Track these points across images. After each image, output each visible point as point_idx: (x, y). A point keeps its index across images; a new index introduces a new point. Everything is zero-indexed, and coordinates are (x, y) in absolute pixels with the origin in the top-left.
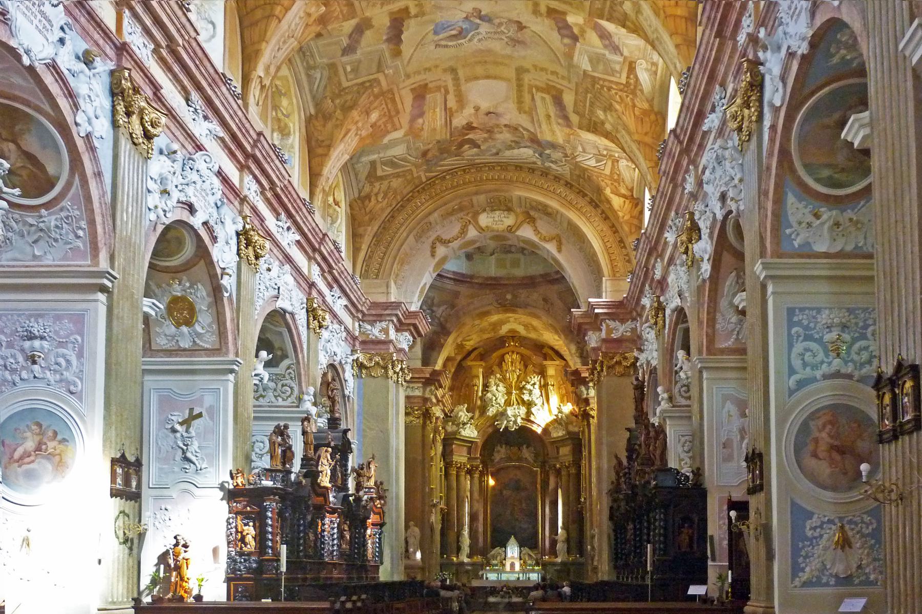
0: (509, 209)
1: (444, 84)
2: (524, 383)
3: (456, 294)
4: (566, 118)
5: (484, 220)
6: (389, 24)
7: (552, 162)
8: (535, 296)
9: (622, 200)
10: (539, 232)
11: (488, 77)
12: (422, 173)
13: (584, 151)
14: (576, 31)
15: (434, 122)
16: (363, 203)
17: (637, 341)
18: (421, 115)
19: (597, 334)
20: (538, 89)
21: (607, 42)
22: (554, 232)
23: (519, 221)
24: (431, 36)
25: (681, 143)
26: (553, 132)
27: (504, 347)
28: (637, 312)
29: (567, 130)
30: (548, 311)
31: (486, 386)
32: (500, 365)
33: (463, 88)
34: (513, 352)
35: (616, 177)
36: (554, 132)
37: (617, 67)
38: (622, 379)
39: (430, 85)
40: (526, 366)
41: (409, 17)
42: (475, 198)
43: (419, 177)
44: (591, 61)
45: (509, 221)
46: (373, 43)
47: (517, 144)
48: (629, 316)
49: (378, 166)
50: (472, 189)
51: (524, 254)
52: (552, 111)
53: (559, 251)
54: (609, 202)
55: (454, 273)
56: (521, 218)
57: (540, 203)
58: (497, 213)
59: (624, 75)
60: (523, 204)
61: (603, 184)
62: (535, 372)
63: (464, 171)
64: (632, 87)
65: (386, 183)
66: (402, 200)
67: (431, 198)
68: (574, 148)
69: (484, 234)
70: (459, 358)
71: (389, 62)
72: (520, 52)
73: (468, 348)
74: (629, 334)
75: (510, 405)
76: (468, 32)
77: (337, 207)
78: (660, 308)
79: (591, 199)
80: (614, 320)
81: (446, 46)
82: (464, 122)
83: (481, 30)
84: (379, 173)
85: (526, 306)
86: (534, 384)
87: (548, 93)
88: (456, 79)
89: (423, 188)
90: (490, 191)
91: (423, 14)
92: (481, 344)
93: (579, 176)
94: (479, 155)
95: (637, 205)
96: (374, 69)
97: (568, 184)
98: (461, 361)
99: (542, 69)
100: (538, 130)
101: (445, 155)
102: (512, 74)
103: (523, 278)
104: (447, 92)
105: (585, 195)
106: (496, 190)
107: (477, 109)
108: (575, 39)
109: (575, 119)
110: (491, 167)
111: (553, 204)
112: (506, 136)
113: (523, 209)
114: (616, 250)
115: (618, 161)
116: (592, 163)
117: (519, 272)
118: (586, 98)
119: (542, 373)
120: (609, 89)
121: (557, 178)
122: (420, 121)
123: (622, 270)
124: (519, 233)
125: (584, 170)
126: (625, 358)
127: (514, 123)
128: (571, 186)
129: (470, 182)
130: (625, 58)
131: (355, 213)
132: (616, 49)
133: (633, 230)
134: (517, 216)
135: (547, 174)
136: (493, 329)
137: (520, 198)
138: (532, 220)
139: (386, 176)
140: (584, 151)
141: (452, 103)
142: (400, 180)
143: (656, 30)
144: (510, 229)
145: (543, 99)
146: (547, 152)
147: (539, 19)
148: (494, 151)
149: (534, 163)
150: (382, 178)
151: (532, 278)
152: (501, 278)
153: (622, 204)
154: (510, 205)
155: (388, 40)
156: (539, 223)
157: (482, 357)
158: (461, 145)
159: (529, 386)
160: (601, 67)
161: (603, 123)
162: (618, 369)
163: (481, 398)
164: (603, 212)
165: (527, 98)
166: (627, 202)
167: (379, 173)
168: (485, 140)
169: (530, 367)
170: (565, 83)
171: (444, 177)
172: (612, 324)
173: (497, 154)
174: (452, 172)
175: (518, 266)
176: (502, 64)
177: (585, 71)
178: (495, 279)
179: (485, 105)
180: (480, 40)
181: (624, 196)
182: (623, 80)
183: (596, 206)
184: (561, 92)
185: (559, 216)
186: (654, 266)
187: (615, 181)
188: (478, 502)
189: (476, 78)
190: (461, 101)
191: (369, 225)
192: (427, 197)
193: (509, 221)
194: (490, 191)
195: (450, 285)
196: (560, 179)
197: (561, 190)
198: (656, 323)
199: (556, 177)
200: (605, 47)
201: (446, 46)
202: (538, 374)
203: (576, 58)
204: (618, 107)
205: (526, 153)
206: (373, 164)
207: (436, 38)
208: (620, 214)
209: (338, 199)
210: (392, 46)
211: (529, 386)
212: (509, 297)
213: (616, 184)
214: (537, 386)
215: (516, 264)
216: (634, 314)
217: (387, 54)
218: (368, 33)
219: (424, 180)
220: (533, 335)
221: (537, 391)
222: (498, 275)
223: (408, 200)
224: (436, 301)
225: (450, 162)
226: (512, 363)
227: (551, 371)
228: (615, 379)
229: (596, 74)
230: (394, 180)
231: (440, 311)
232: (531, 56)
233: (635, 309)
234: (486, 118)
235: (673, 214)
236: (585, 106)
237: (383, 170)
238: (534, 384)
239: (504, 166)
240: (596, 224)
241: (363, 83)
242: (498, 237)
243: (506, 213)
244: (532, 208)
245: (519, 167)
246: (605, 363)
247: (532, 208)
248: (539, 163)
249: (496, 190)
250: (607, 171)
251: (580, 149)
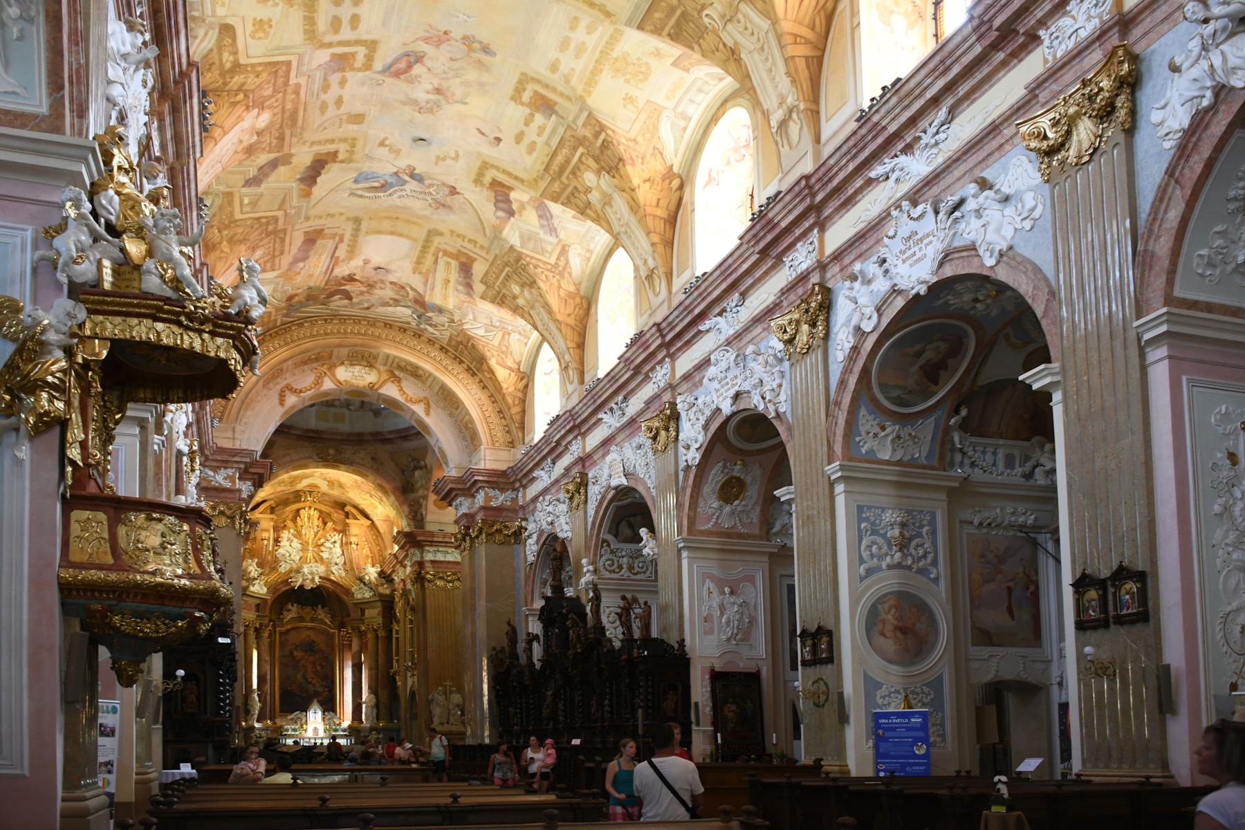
0: (371, 366)
1: (340, 232)
4: (469, 286)
6: (309, 164)
7: (431, 325)
11: (392, 233)
13: (475, 319)
14: (515, 206)
15: (314, 271)
17: (524, 511)
18: (304, 259)
20: (446, 253)
21: (545, 223)
23: (382, 379)
24: (350, 184)
25: (663, 336)
26: (445, 297)
29: (463, 297)
33: (360, 239)
36: (445, 293)
37: (549, 248)
39: (327, 231)
41: (335, 161)
44: (521, 237)
46: (284, 179)
47: (396, 302)
52: (454, 275)
53: (428, 414)
56: (385, 376)
57: (411, 364)
58: (357, 368)
59: (554, 256)
64: (560, 269)
68: (464, 315)
71: (295, 201)
72: (442, 214)
76: (391, 185)
78: (583, 484)
81: (361, 196)
82: (347, 273)
83: (407, 187)
87: (457, 259)
88: (357, 230)
90: (356, 345)
91: (350, 160)
96: (276, 207)
97: (442, 348)
99: (459, 236)
100: (428, 292)
102: (422, 235)
104: (341, 240)
105: (461, 362)
106: (362, 346)
107: (366, 262)
108: (511, 213)
109: (479, 288)
110: (357, 320)
111: (427, 366)
112: (389, 293)
114: (494, 419)
118: (502, 271)
120: (536, 267)
121: (431, 342)
122: (301, 264)
127: (403, 281)
128: (447, 352)
129: (332, 333)
130: (560, 241)
132: (553, 230)
134: (380, 373)
137: (388, 356)
138: (398, 380)
140: (475, 319)
141: (342, 252)
143: (627, 225)
144: (372, 386)
145: (448, 264)
146: (430, 314)
147: (478, 189)
148: (366, 305)
154: (373, 361)
155: (301, 180)
156: (405, 384)
158: (332, 295)
160: (531, 245)
161: (515, 297)
165: (429, 259)
168: (362, 293)
170: (483, 253)
172: (491, 492)
174: (312, 320)
176: (415, 223)
177: (512, 247)
179: (377, 260)
180: (400, 197)
182: (553, 261)
183: (474, 374)
184: (473, 260)
185: (430, 380)
186: (570, 442)
189: (379, 232)
190: (353, 250)
197: (435, 353)
198: (571, 499)
200: (542, 226)
201: (361, 196)
203: (505, 233)
204: (541, 285)
205: (404, 313)
207: (355, 186)
210: (302, 187)
216: (518, 485)
217: (295, 194)
218: (282, 169)
225: (313, 309)
229: (524, 251)
232: (455, 221)
233: (520, 480)
234: (374, 272)
235: (620, 398)
236: (498, 277)
239: (373, 323)
240: (473, 392)
241: (258, 219)
244: (400, 368)
245: (388, 325)
247: (400, 368)
251: (471, 317)
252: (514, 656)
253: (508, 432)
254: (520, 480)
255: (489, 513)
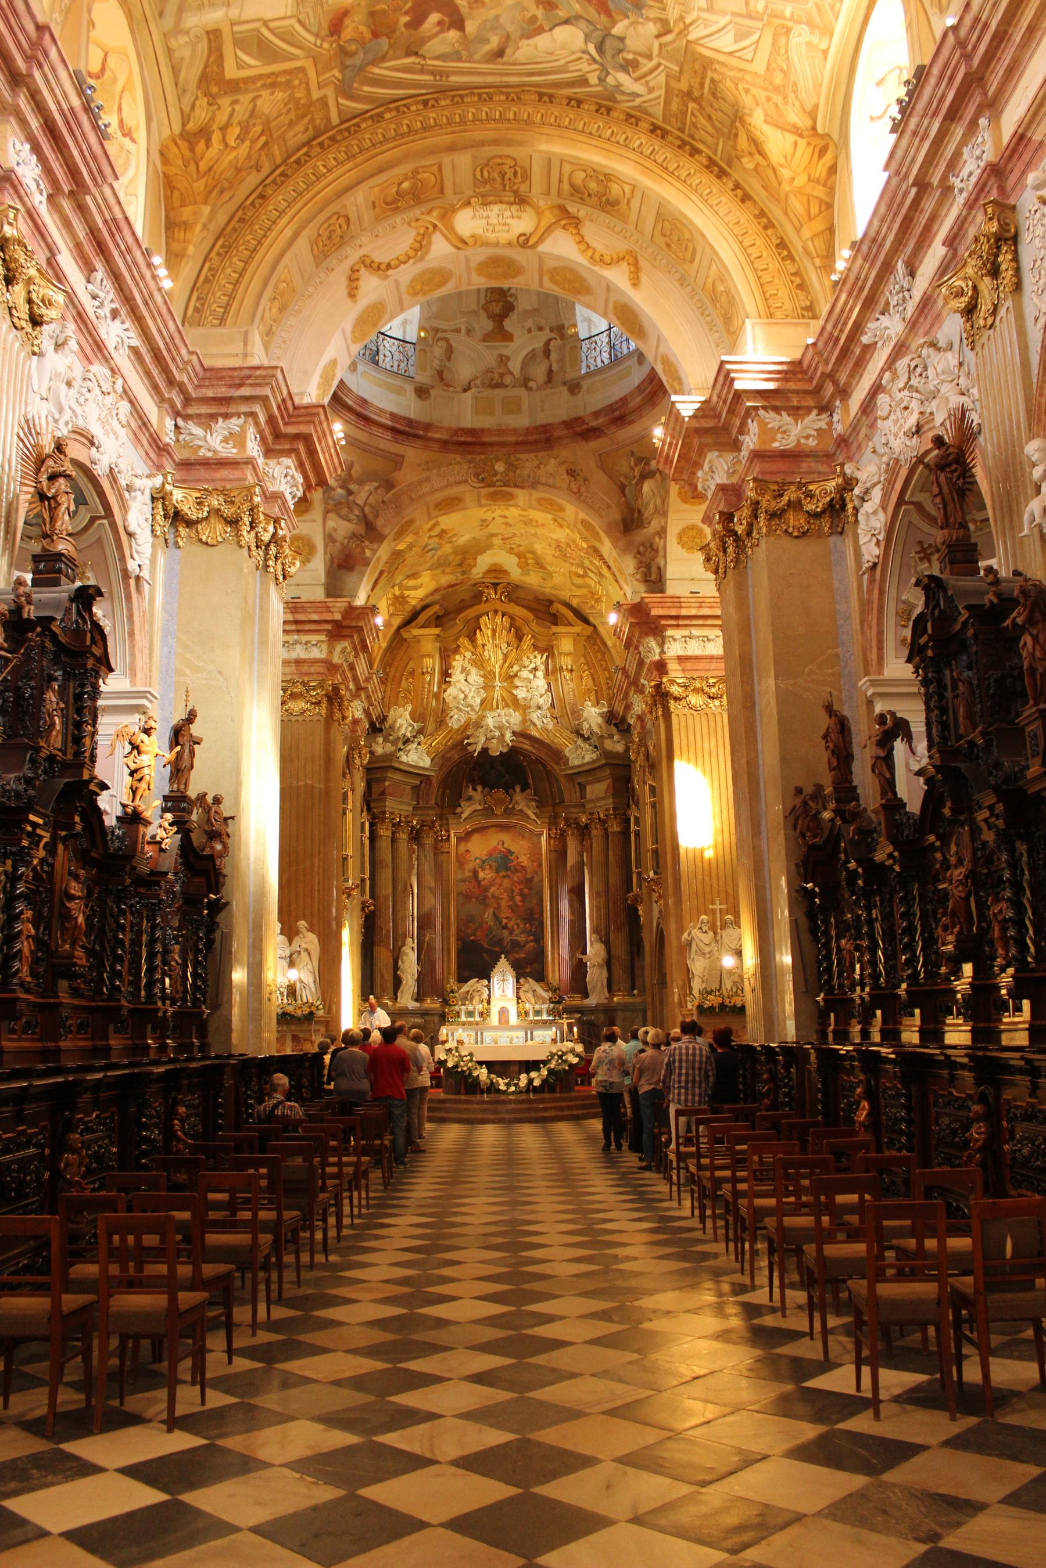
0: (521, 201)
2: (516, 668)
3: (397, 461)
5: (466, 222)
8: (552, 466)
9: (790, 138)
10: (588, 246)
12: (330, 92)
16: (192, 150)
19: (730, 457)
22: (621, 246)
23: (544, 225)
27: (480, 602)
28: (836, 383)
30: (578, 495)
31: (446, 674)
32: (472, 638)
34: (496, 612)
35: (779, 80)
38: (803, 542)
40: (520, 638)
42: (447, 160)
43: (323, 101)
45: (523, 223)
48: (810, 402)
49: (228, 49)
50: (442, 139)
51: (530, 389)
53: (636, 283)
54: (757, 147)
55: (393, 416)
56: (549, 218)
58: (496, 208)
60: (554, 190)
61: (747, 100)
62: (535, 647)
63: (425, 103)
65: (245, 99)
66: (284, 162)
67: (350, 157)
69: (468, 252)
70: (397, 622)
73: (413, 602)
74: (812, 443)
75: (491, 709)
77: (127, 141)
79: (710, 159)
80: (776, 409)
84: (231, 72)
85: (533, 486)
86: (536, 669)
89: (332, 139)
90: (482, 144)
92: (437, 597)
93: (689, 95)
94: (457, 56)
95: (823, 151)
97: (654, 129)
98: (399, 628)
101: (384, 43)
103: (529, 431)
105: (695, 152)
110: (484, 93)
111: (624, 168)
113: (553, 200)
114: (770, 261)
115: (788, 30)
116: (726, 42)
117: (521, 421)
119: (548, 650)
123: (788, 306)
124: (546, 247)
125: (707, 64)
126: (810, 495)
131: (172, 171)
133: (814, 211)
134: (539, 213)
135: (609, 110)
136: (460, 565)
138: (573, 223)
139: (246, 80)
142: (280, 95)
144: (524, 242)
146: (618, 30)
148: (495, 41)
149: (583, 81)
150: (234, 87)
151: (546, 428)
152: (482, 430)
153: (790, 149)
154: (523, 188)
156: (588, 230)
157: (438, 621)
159: (525, 674)
162: (795, 520)
163: (437, 696)
164: (737, 186)
166: (802, 143)
167: (231, 72)
169: (527, 641)
171: (380, 115)
172: (773, 420)
173: (500, 53)
175: (518, 410)
178: (472, 432)
181: (797, 131)
183: (722, 174)
187: (777, 90)
188: (431, 889)
191: (206, 203)
192: (342, 156)
193: (523, 223)
194: (482, 144)
195: (385, 442)
196: (638, 120)
197: (641, 139)
199: (629, 116)
202: (542, 651)
206: (214, 35)
208: (785, 173)
209: (129, 122)
211: (525, 674)
212: (500, 467)
213: (777, 99)
214: (540, 674)
215: (512, 407)
216: (829, 389)
219: (335, 120)
220: (533, 580)
221: (541, 682)
222: (478, 425)
223: (298, 162)
224: (356, 472)
226: (494, 631)
227: (566, 645)
228: (787, 542)
230: (265, 93)
231: (363, 494)
237: (240, 65)
238: (536, 669)
239: (514, 94)
240: (723, 210)
242: (496, 264)
243: (514, 208)
244: (578, 192)
245: (545, 96)
246: (764, 504)
248: (593, 79)
249: (495, 142)
250: (760, 66)
252: (846, 791)
253: (801, 287)
254: (831, 376)
255: (771, 466)
